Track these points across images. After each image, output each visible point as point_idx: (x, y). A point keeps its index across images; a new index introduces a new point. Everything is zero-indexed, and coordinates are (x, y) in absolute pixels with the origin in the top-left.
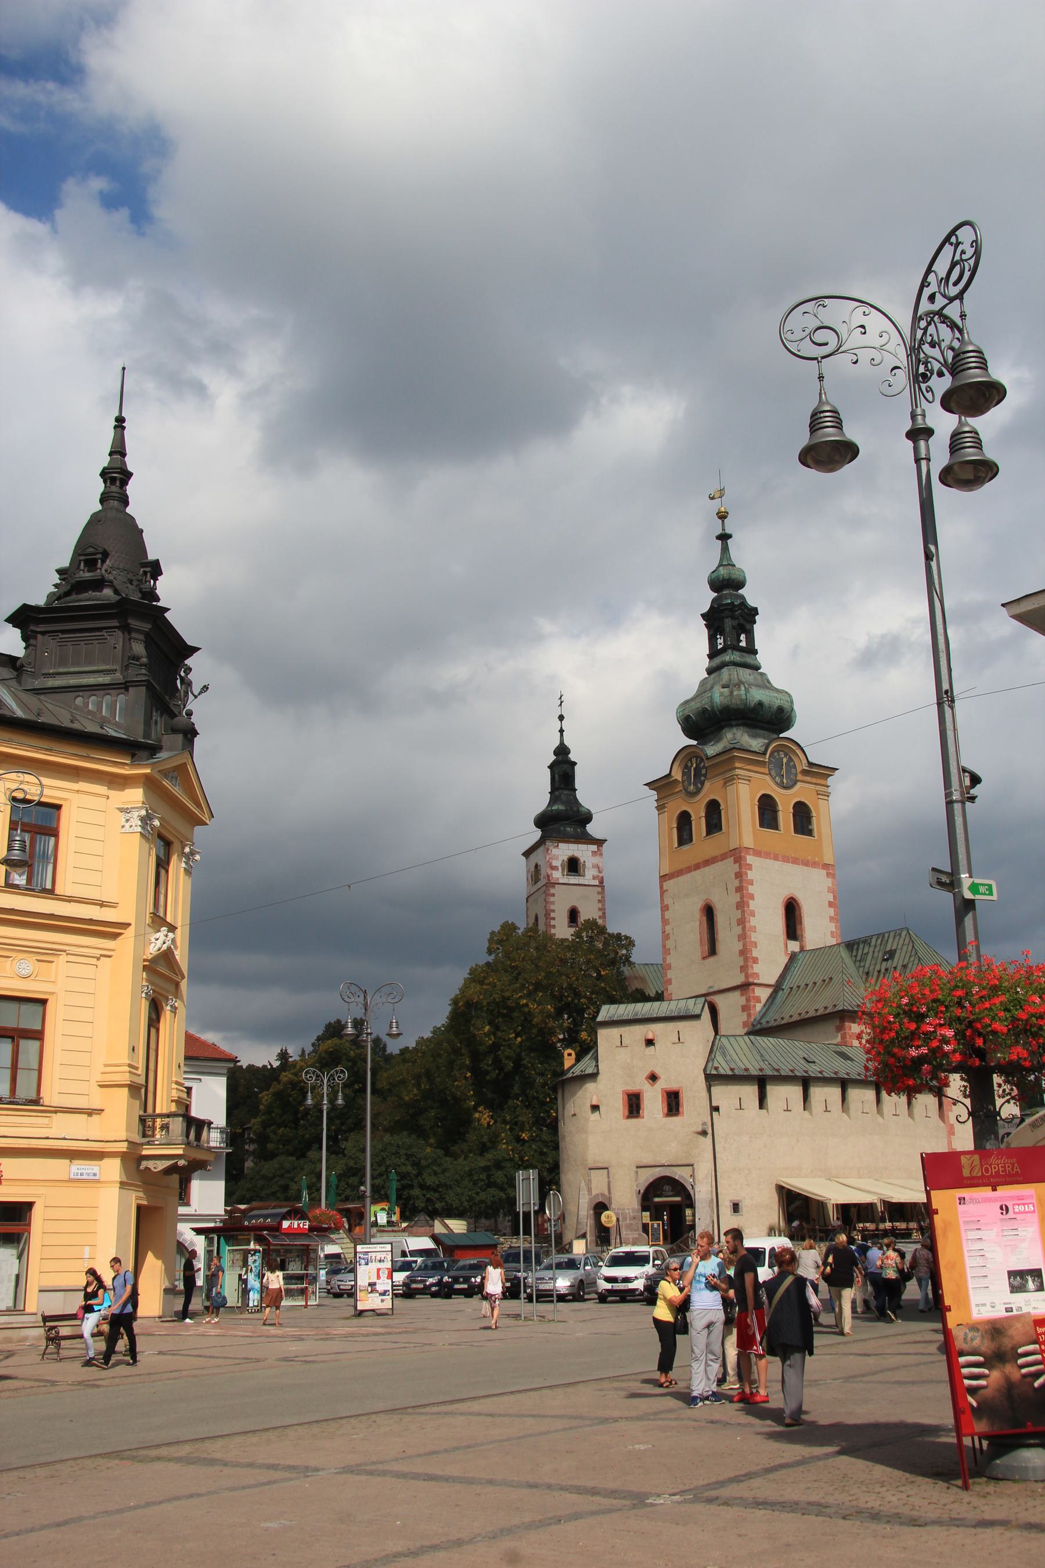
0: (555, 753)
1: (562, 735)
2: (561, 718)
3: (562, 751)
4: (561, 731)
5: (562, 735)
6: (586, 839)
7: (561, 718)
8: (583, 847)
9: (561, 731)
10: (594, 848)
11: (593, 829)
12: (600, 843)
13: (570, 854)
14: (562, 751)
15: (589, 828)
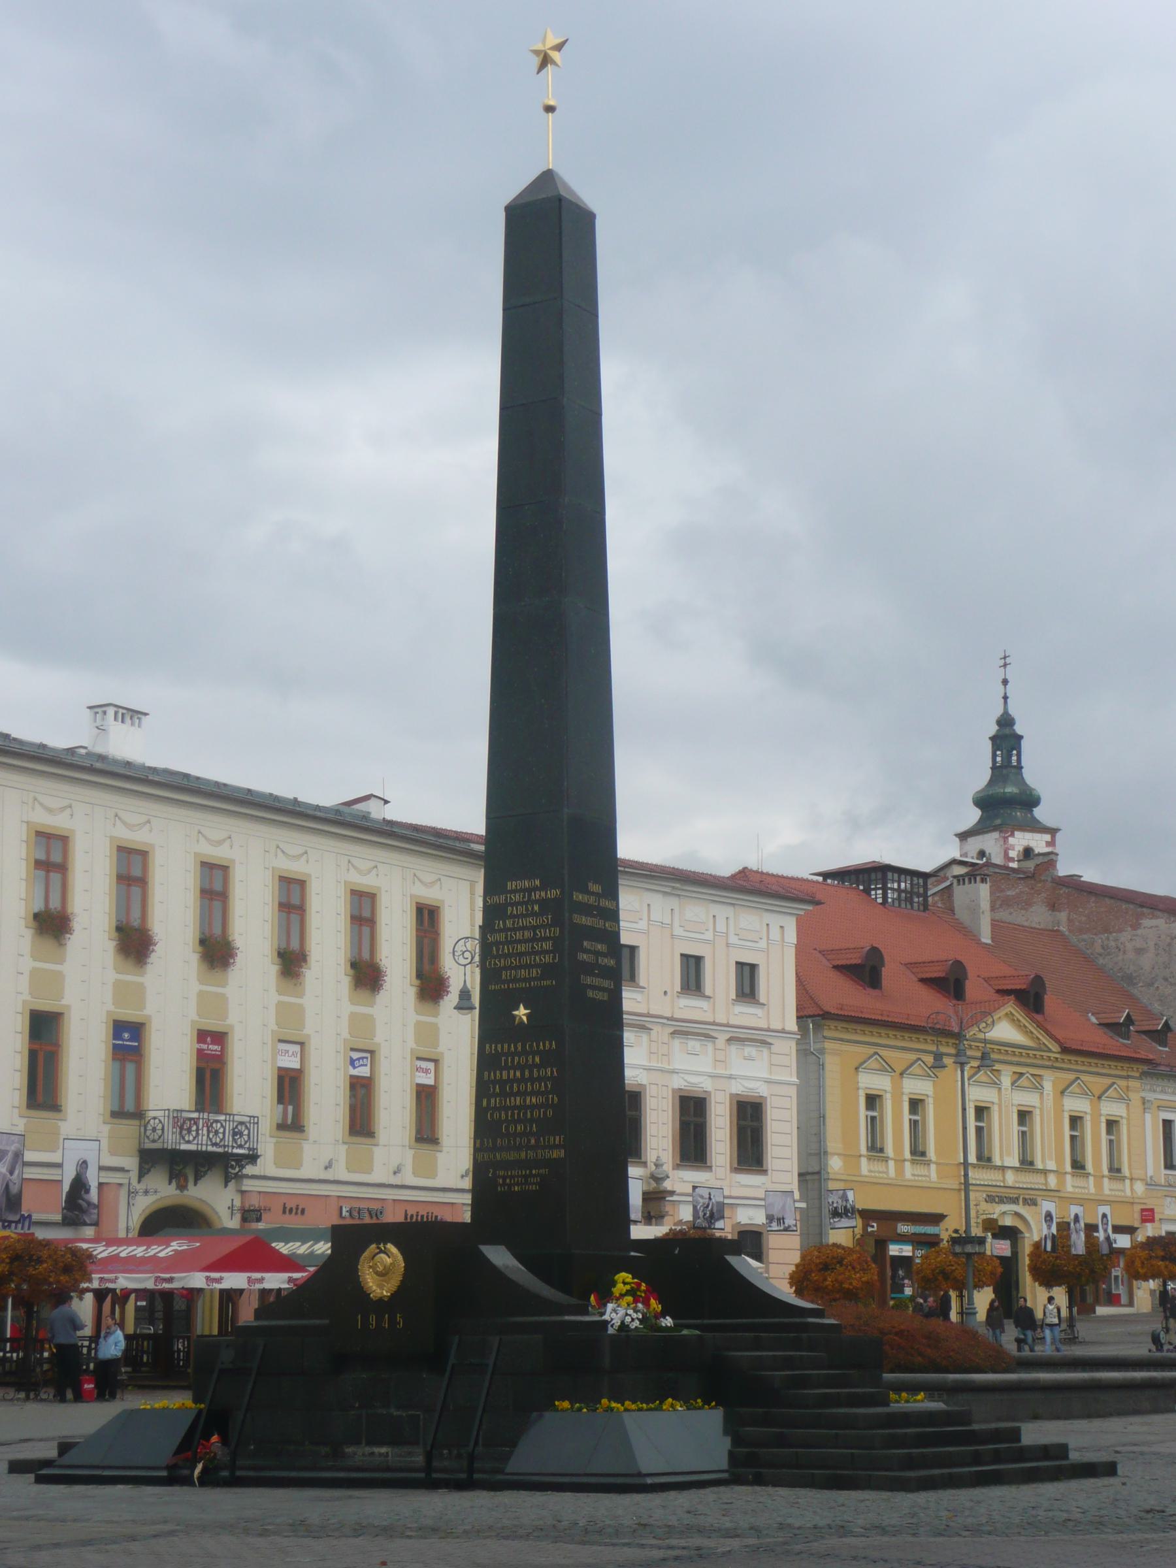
0: (999, 723)
1: (1006, 703)
2: (1005, 682)
3: (1006, 722)
4: (1005, 698)
5: (1006, 703)
6: (1036, 827)
7: (1005, 682)
8: (1037, 836)
9: (1005, 698)
10: (1048, 837)
11: (1040, 813)
12: (1053, 832)
13: (1025, 843)
14: (1006, 722)
15: (1038, 812)
